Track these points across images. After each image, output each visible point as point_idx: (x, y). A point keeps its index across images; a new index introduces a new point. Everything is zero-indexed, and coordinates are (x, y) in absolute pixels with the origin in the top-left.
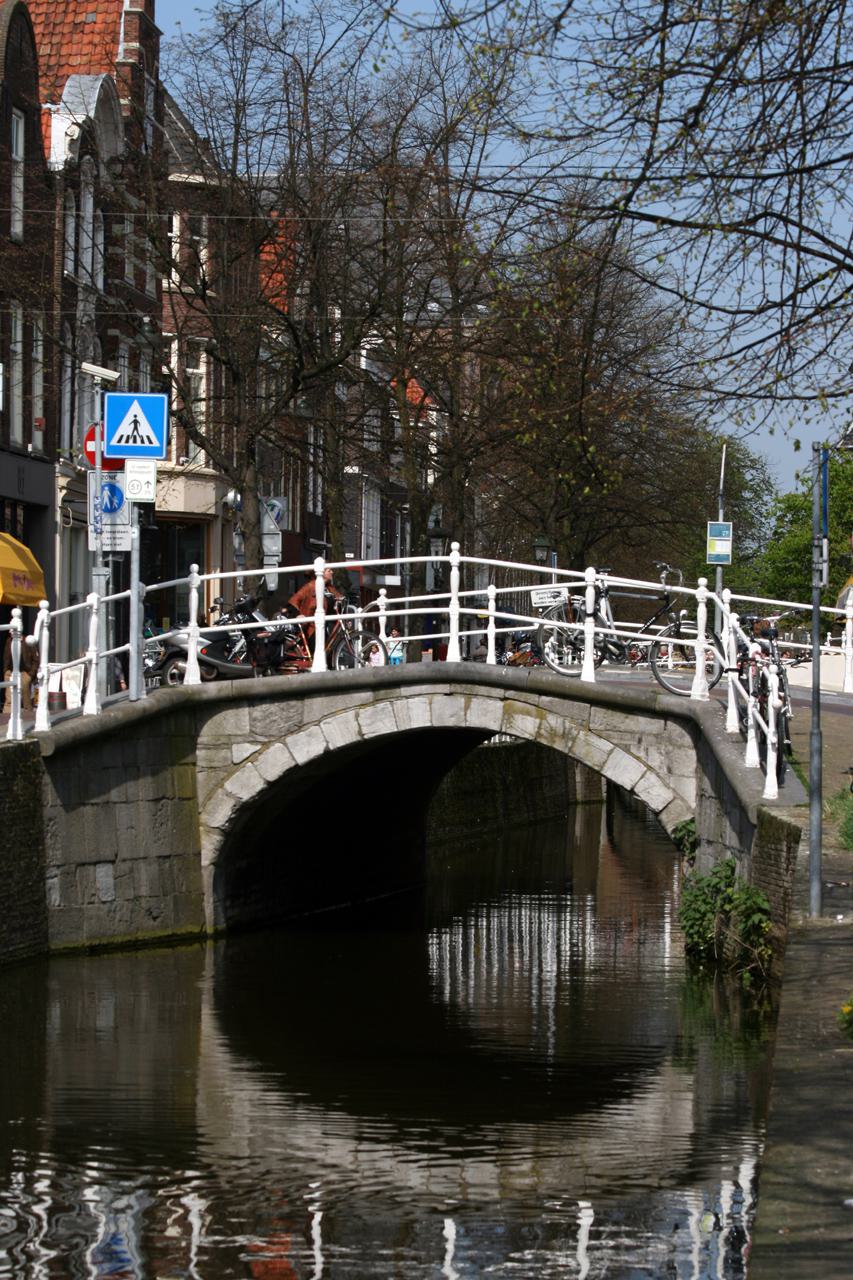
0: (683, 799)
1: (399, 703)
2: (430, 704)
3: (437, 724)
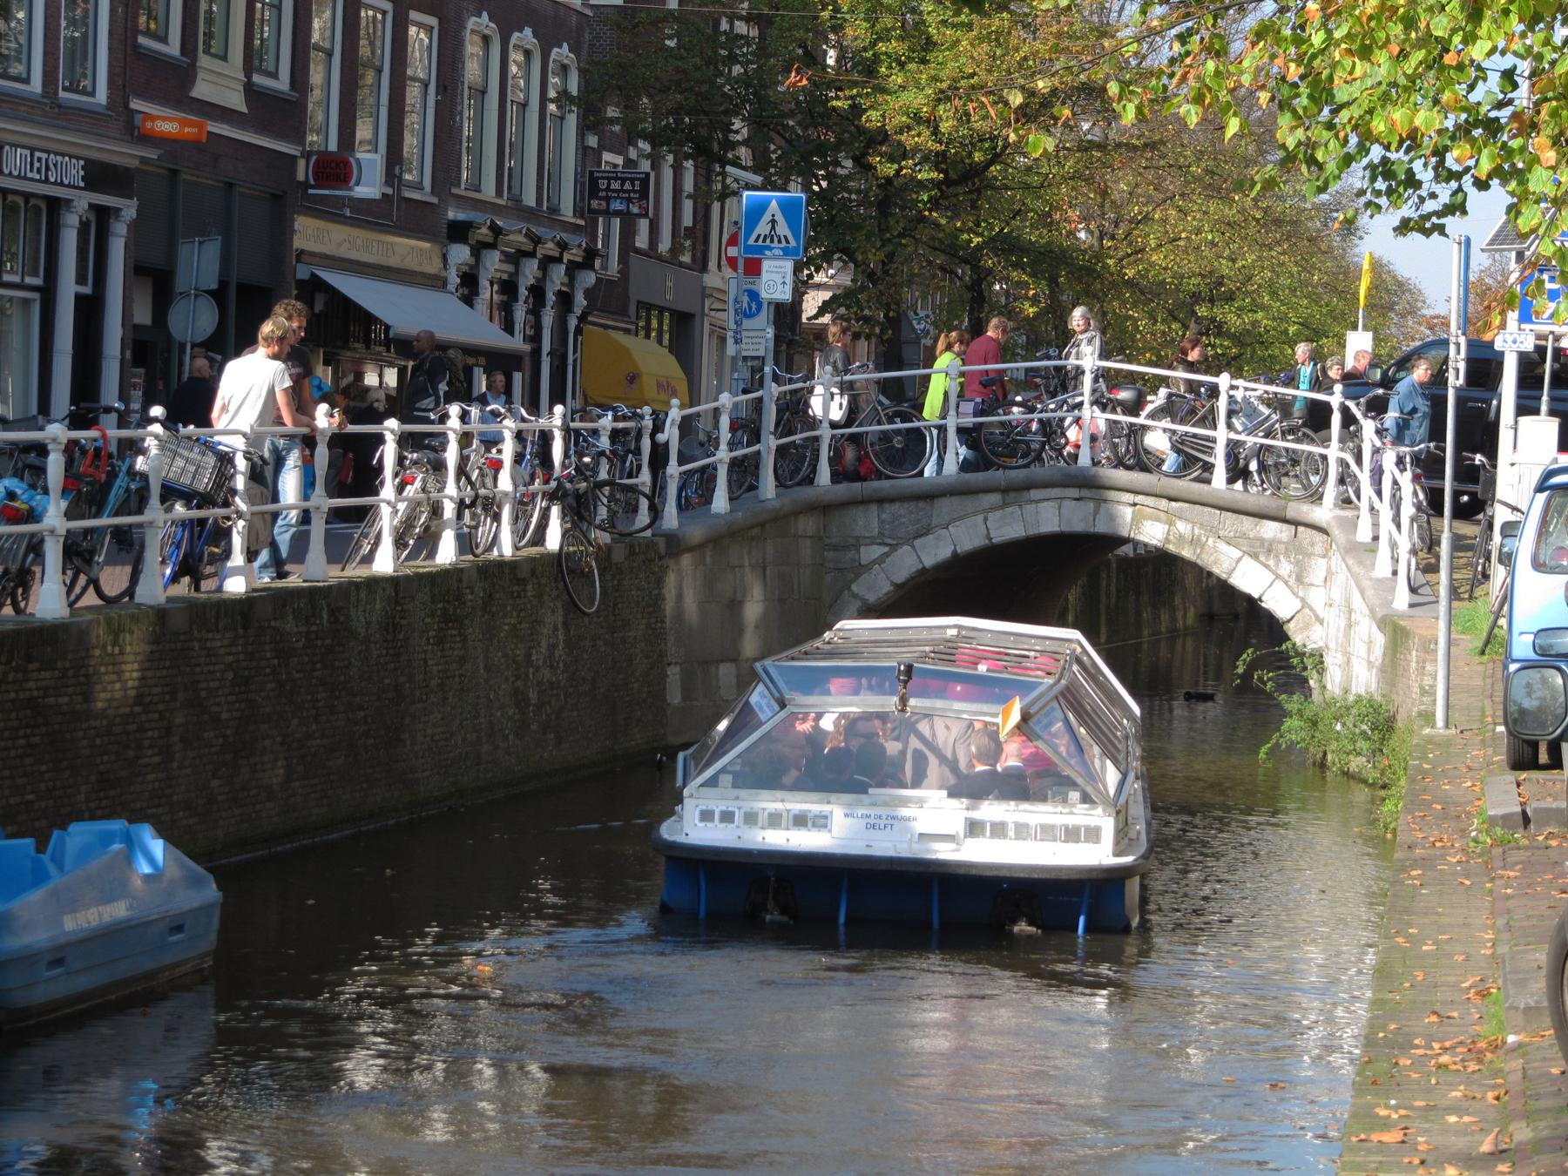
0: (1311, 609)
1: (1028, 508)
2: (1060, 508)
3: (1066, 528)
